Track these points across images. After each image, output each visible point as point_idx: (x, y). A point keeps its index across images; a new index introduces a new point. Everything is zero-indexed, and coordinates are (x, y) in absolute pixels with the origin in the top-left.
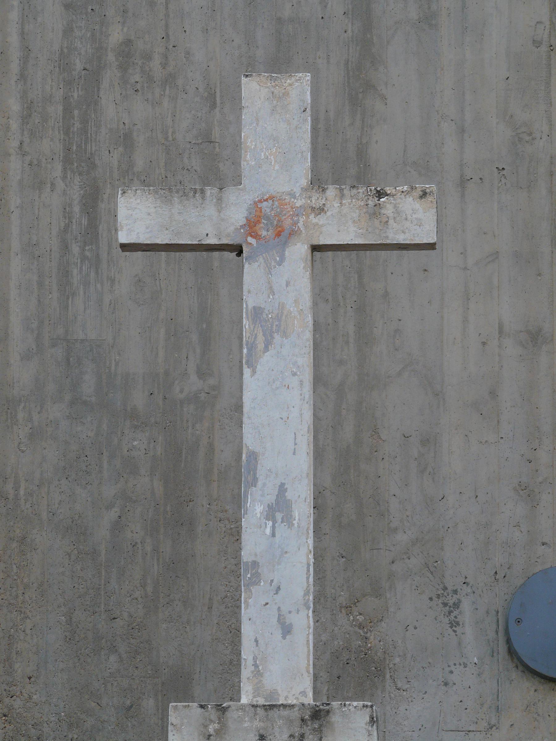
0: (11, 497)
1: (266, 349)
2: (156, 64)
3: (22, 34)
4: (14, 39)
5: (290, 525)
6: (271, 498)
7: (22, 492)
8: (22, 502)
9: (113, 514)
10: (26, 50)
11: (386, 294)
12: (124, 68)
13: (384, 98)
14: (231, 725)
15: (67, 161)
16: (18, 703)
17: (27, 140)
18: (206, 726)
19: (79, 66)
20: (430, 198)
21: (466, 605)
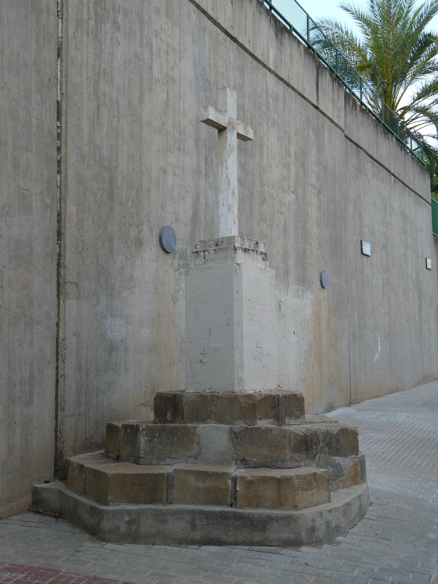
0: (83, 182)
1: (231, 155)
2: (109, 77)
3: (87, 57)
4: (85, 57)
5: (235, 198)
6: (232, 191)
7: (85, 181)
8: (85, 184)
9: (101, 192)
10: (87, 61)
11: (144, 153)
12: (104, 76)
13: (144, 105)
14: (245, 243)
15: (94, 95)
16: (84, 238)
17: (87, 86)
18: (241, 242)
19: (97, 71)
20: (253, 129)
21: (154, 231)
